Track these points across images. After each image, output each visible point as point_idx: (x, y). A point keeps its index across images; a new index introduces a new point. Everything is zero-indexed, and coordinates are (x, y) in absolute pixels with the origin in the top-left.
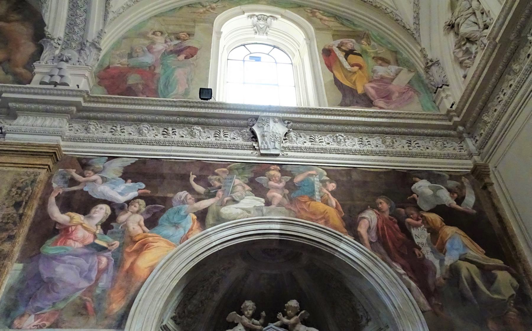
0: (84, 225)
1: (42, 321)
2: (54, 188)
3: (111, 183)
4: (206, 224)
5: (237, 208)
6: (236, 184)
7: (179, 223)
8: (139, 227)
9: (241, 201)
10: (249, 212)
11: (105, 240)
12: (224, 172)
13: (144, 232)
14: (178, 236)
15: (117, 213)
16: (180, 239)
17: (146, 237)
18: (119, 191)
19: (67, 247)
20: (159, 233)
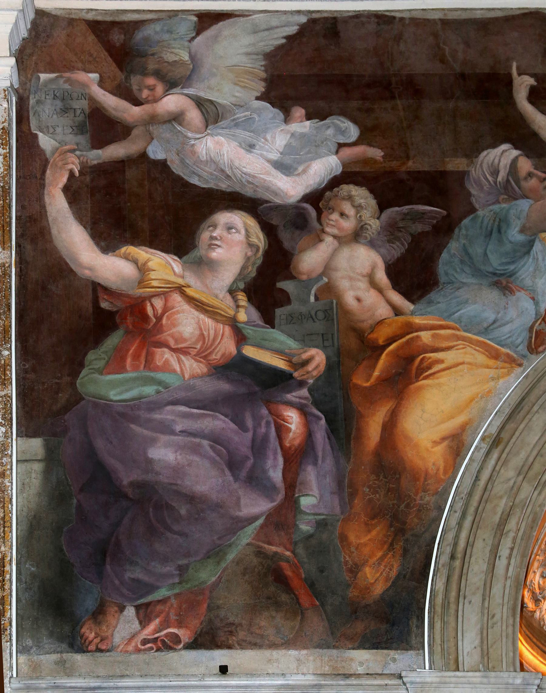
0: (188, 291)
1: (165, 624)
2: (48, 153)
3: (237, 125)
11: (276, 345)
13: (397, 311)
14: (517, 323)
15: (287, 245)
17: (410, 328)
18: (274, 156)
19: (159, 376)
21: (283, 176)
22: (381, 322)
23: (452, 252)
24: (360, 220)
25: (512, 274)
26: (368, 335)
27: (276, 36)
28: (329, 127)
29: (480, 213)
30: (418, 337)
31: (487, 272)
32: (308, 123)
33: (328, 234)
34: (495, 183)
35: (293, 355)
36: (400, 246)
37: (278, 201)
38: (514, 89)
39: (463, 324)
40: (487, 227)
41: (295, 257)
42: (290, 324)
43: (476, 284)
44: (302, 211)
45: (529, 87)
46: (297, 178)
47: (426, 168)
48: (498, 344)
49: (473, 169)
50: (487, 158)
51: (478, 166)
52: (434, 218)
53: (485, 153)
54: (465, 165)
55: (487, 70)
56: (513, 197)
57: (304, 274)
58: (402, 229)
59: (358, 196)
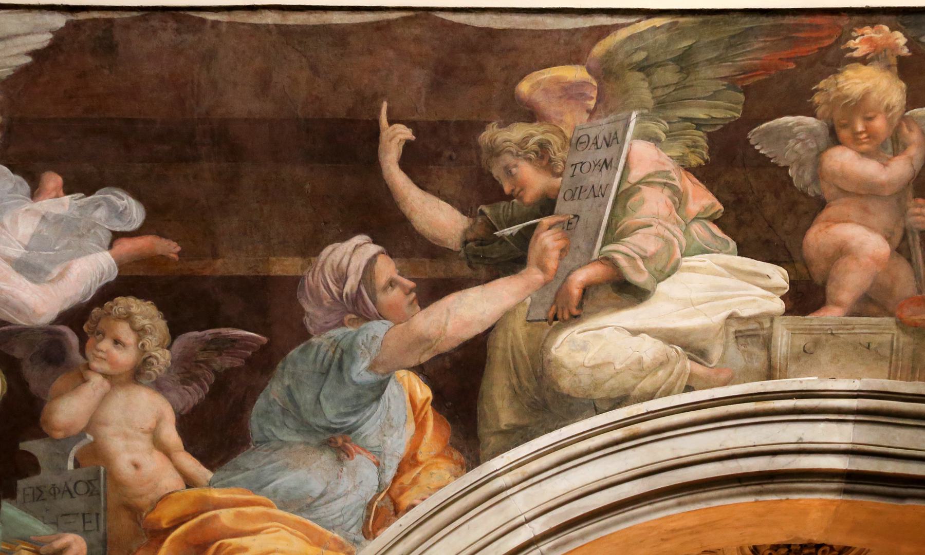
4: (482, 430)
5: (635, 333)
6: (636, 175)
7: (351, 430)
8: (158, 456)
9: (662, 287)
10: (699, 354)
12: (571, 92)
13: (190, 482)
14: (353, 499)
15: (34, 386)
16: (361, 512)
17: (205, 505)
18: (16, 252)
20: (259, 490)
21: (29, 283)
22: (164, 498)
23: (272, 397)
24: (142, 349)
25: (351, 430)
26: (146, 516)
27: (15, 51)
28: (99, 206)
29: (314, 340)
30: (216, 517)
31: (318, 426)
32: (67, 199)
33: (95, 371)
34: (341, 295)
35: (42, 544)
36: (198, 388)
37: (21, 322)
38: (381, 146)
39: (278, 499)
40: (323, 360)
41: (47, 406)
42: (37, 500)
43: (301, 443)
44: (57, 337)
45: (403, 143)
46: (50, 288)
47: (242, 272)
48: (323, 526)
49: (310, 274)
50: (332, 256)
51: (318, 269)
52: (247, 347)
53: (329, 249)
54: (299, 268)
55: (343, 114)
56: (365, 317)
57: (60, 430)
58: (202, 365)
59: (140, 314)
